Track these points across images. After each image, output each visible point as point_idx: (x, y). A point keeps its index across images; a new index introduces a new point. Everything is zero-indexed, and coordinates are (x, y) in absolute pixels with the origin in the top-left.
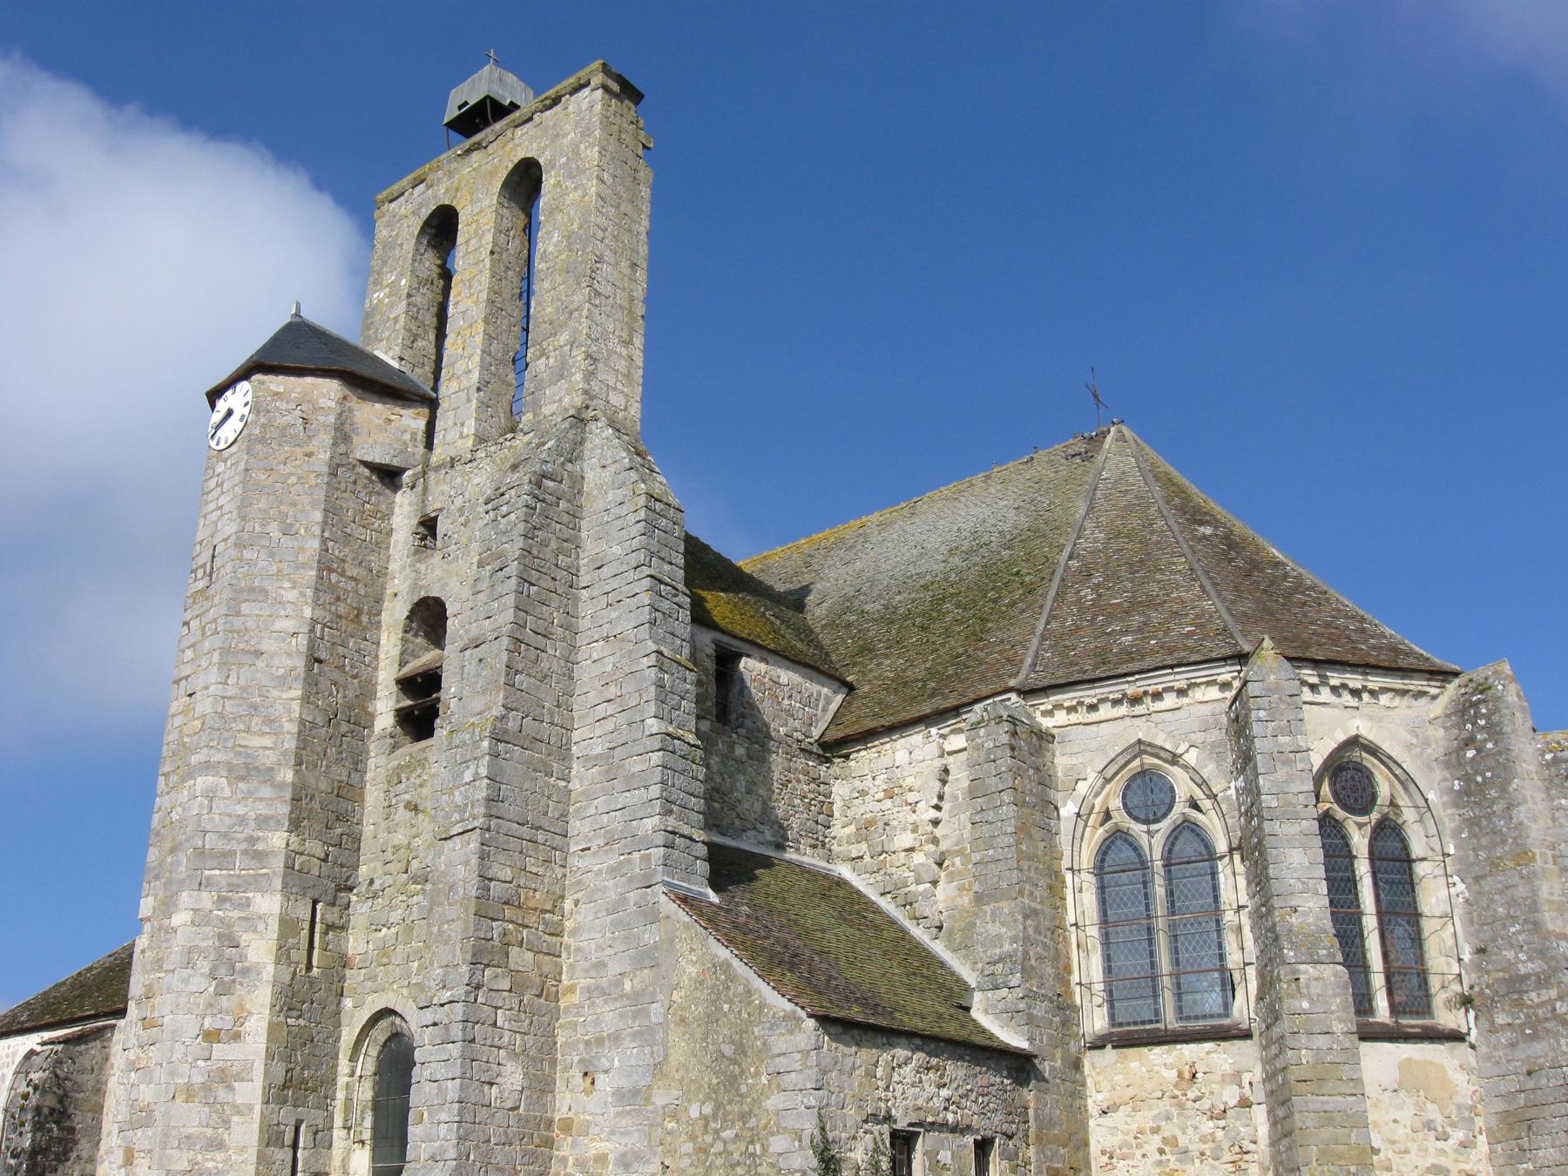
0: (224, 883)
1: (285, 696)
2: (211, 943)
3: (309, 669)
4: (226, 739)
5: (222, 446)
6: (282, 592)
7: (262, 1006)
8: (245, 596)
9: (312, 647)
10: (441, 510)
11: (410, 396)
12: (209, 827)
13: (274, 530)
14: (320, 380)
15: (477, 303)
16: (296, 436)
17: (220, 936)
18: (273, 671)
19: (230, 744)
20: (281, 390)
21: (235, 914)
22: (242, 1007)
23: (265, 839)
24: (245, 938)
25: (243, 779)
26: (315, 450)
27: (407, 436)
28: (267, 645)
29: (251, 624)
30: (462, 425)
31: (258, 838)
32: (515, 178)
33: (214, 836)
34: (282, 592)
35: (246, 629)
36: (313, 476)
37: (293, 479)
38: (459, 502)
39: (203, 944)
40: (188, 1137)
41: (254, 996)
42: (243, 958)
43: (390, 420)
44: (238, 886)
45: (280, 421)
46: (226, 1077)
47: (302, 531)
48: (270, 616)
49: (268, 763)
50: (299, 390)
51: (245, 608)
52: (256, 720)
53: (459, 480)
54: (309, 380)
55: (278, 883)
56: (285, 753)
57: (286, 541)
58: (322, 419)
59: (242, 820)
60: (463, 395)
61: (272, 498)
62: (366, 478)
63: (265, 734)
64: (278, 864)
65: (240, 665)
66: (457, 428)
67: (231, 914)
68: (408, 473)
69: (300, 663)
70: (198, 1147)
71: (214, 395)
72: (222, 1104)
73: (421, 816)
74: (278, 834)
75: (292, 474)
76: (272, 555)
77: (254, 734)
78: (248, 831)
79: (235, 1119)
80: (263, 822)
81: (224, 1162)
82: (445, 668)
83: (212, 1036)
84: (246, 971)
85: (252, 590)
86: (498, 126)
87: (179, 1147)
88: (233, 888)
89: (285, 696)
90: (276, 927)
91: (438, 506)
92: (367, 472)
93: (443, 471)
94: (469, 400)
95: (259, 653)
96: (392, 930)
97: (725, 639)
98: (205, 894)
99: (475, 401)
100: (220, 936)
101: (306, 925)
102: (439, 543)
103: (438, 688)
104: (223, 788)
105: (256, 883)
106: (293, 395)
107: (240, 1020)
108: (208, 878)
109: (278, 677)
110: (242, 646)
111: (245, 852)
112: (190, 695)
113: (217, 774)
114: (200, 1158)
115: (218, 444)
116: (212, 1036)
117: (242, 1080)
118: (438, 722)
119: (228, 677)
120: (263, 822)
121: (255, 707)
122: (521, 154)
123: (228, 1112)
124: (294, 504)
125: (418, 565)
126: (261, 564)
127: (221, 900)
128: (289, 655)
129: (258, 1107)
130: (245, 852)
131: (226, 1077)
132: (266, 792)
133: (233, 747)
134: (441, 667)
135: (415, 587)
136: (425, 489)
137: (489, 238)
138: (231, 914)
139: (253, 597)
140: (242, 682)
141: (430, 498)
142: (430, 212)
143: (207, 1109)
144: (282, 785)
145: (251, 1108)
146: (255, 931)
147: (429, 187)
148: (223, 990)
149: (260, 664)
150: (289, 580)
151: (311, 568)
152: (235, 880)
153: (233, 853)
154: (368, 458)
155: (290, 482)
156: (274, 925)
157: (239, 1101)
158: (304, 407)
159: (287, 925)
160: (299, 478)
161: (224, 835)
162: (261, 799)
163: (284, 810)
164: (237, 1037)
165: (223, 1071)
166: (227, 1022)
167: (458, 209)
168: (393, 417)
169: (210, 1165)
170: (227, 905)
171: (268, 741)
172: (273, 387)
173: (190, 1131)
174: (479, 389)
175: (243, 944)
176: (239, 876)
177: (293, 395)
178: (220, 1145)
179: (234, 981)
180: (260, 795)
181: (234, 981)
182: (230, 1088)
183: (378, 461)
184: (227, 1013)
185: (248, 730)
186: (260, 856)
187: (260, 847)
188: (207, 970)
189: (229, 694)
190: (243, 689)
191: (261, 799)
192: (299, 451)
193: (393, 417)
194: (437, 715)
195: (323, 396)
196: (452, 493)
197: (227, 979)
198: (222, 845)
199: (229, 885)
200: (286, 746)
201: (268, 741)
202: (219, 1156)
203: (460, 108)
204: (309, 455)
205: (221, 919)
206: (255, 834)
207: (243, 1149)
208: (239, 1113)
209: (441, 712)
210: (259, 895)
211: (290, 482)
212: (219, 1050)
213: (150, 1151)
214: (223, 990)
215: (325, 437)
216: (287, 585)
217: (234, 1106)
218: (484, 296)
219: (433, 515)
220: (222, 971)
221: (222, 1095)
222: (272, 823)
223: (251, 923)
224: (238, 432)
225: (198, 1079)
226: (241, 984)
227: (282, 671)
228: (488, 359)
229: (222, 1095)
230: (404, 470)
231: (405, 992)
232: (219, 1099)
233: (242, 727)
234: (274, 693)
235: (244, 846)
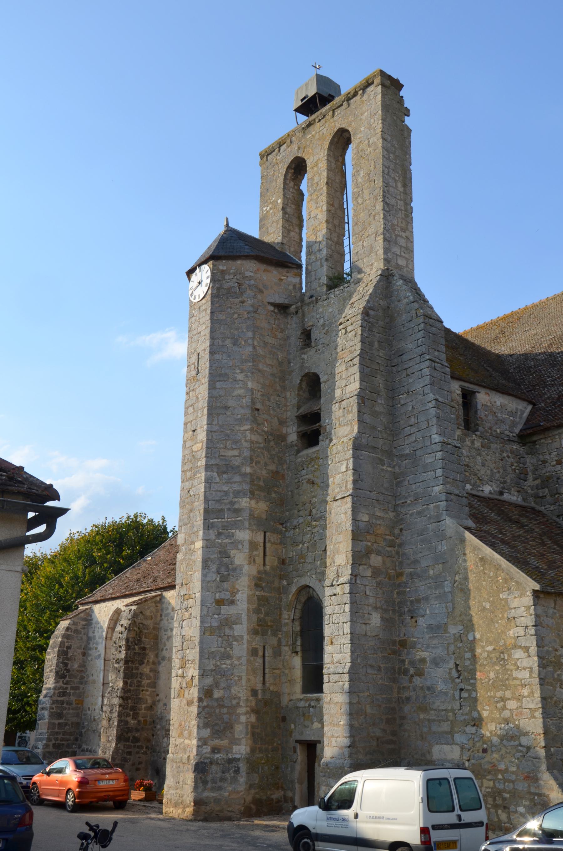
0: (220, 525)
1: (242, 429)
2: (216, 556)
3: (254, 416)
4: (215, 453)
5: (197, 300)
6: (236, 375)
7: (244, 586)
8: (218, 379)
9: (253, 403)
10: (313, 326)
11: (290, 265)
12: (210, 498)
13: (228, 342)
14: (244, 262)
15: (322, 211)
16: (235, 293)
17: (220, 552)
18: (235, 416)
19: (217, 455)
20: (225, 268)
21: (226, 541)
22: (234, 587)
23: (238, 502)
24: (233, 552)
25: (224, 473)
26: (246, 299)
27: (291, 287)
28: (231, 403)
29: (222, 393)
30: (320, 279)
31: (235, 502)
32: (336, 139)
33: (213, 502)
34: (236, 375)
35: (220, 396)
36: (246, 313)
37: (236, 316)
38: (322, 321)
39: (212, 557)
40: (213, 653)
41: (239, 581)
42: (232, 563)
43: (282, 280)
44: (227, 526)
45: (226, 286)
46: (228, 623)
47: (243, 343)
48: (231, 388)
49: (237, 464)
50: (234, 268)
51: (218, 385)
52: (229, 442)
53: (321, 310)
54: (239, 262)
55: (246, 524)
56: (245, 458)
57: (236, 348)
58: (247, 282)
59: (226, 493)
60: (318, 263)
61: (226, 326)
62: (272, 311)
63: (234, 449)
64: (246, 515)
65: (218, 415)
66: (317, 281)
67: (224, 541)
68: (293, 307)
69: (248, 412)
70: (218, 658)
71: (190, 272)
72: (228, 636)
73: (316, 486)
74: (245, 500)
75: (234, 313)
76: (229, 356)
77: (229, 449)
78: (230, 499)
79: (235, 643)
80: (237, 494)
81: (231, 665)
82: (323, 409)
83: (220, 602)
84: (235, 570)
85: (220, 375)
86: (323, 110)
87: (208, 658)
88: (225, 527)
89: (242, 429)
90: (248, 547)
91: (311, 324)
92: (272, 308)
93: (312, 305)
94: (322, 266)
95: (226, 408)
96: (305, 545)
97: (466, 385)
98: (211, 532)
99: (325, 267)
100: (220, 552)
101: (262, 544)
102: (313, 344)
103: (319, 420)
104: (215, 478)
105: (237, 525)
106: (231, 271)
107: (234, 593)
108: (212, 523)
109: (238, 419)
110: (218, 405)
111: (229, 509)
112: (194, 431)
113: (212, 471)
114: (219, 663)
115: (195, 299)
116: (220, 602)
117: (237, 624)
118: (321, 437)
119: (213, 421)
120: (237, 494)
121: (228, 435)
122: (338, 126)
123: (231, 640)
124: (237, 329)
125: (303, 356)
126: (224, 361)
127: (219, 534)
128: (242, 407)
129: (245, 637)
130: (229, 509)
131: (228, 623)
132: (237, 478)
133: (219, 457)
134: (320, 409)
135: (302, 367)
136: (303, 315)
137: (325, 174)
138: (224, 541)
139: (221, 379)
140: (220, 423)
141: (306, 320)
142: (290, 161)
143: (220, 639)
144: (245, 474)
145: (242, 637)
146: (238, 549)
147: (288, 146)
148: (224, 579)
149: (229, 413)
150: (239, 369)
151: (250, 362)
152: (225, 524)
153: (222, 510)
154: (272, 301)
155: (234, 317)
156: (246, 545)
157: (236, 634)
158: (238, 277)
159: (253, 545)
160: (239, 315)
161: (218, 501)
162: (235, 482)
163: (246, 487)
164: (232, 602)
165: (226, 619)
166: (226, 595)
167: (306, 158)
168: (283, 278)
169: (224, 666)
170: (223, 537)
171: (236, 453)
172: (221, 267)
173: (213, 650)
174: (327, 260)
175: (232, 556)
176: (227, 522)
177: (231, 271)
178: (229, 657)
179: (229, 575)
180: (235, 480)
181: (229, 575)
182: (231, 628)
183: (277, 302)
184: (227, 591)
185: (225, 448)
186: (237, 511)
187: (236, 506)
188: (215, 570)
189: (214, 430)
190: (221, 426)
191: (235, 482)
192: (237, 301)
193: (283, 278)
194: (320, 434)
195: (247, 270)
196: (318, 316)
197: (226, 573)
198: (218, 506)
199: (223, 526)
200: (245, 454)
201: (236, 453)
202: (228, 662)
203: (302, 100)
204: (243, 302)
205: (220, 544)
206: (233, 500)
207: (239, 658)
208: (236, 640)
209: (322, 432)
210: (237, 531)
211: (234, 317)
212: (224, 609)
213: (194, 660)
214: (224, 579)
215: (250, 292)
216: (238, 371)
217: (233, 636)
218: (325, 208)
219: (308, 329)
220: (223, 569)
221: (227, 631)
222: (241, 494)
223: (236, 544)
224: (205, 292)
225: (215, 624)
226: (233, 576)
227: (239, 416)
228: (330, 242)
229: (227, 631)
230: (291, 305)
231: (314, 576)
232: (226, 634)
233: (222, 446)
234: (237, 428)
235: (229, 506)
